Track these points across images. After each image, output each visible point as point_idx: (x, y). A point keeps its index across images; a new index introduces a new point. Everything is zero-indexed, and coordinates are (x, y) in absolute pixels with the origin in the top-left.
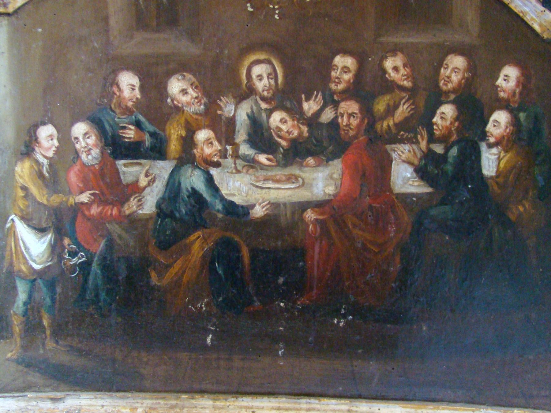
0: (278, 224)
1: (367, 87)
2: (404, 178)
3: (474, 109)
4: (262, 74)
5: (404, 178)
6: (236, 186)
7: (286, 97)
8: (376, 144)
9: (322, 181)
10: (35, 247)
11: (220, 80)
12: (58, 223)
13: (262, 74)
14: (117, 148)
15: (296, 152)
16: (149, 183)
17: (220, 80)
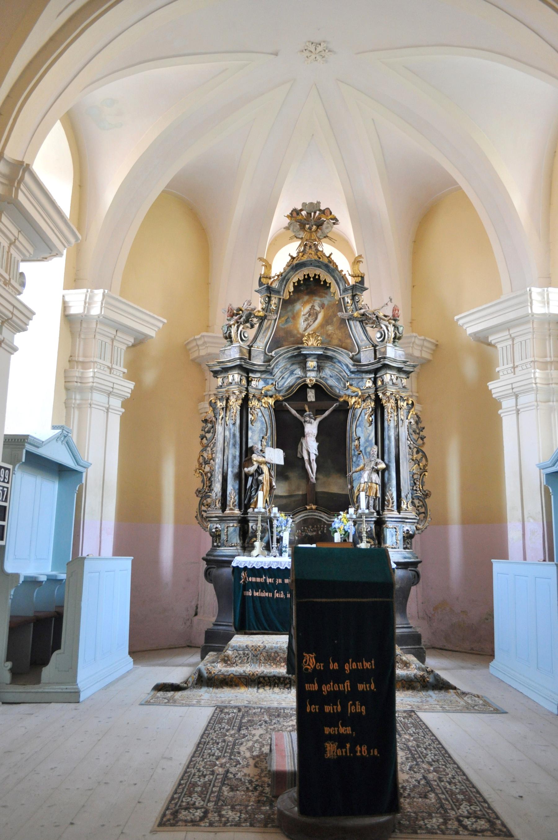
0: (312, 536)
1: (317, 527)
2: (320, 533)
3: (324, 528)
4: (310, 527)
5: (320, 533)
6: (309, 534)
7: (312, 528)
8: (318, 531)
9: (314, 533)
10: (297, 538)
11: (308, 527)
12: (298, 536)
13: (310, 527)
14: (302, 532)
15: (313, 532)
16: (304, 534)
17: (308, 527)
